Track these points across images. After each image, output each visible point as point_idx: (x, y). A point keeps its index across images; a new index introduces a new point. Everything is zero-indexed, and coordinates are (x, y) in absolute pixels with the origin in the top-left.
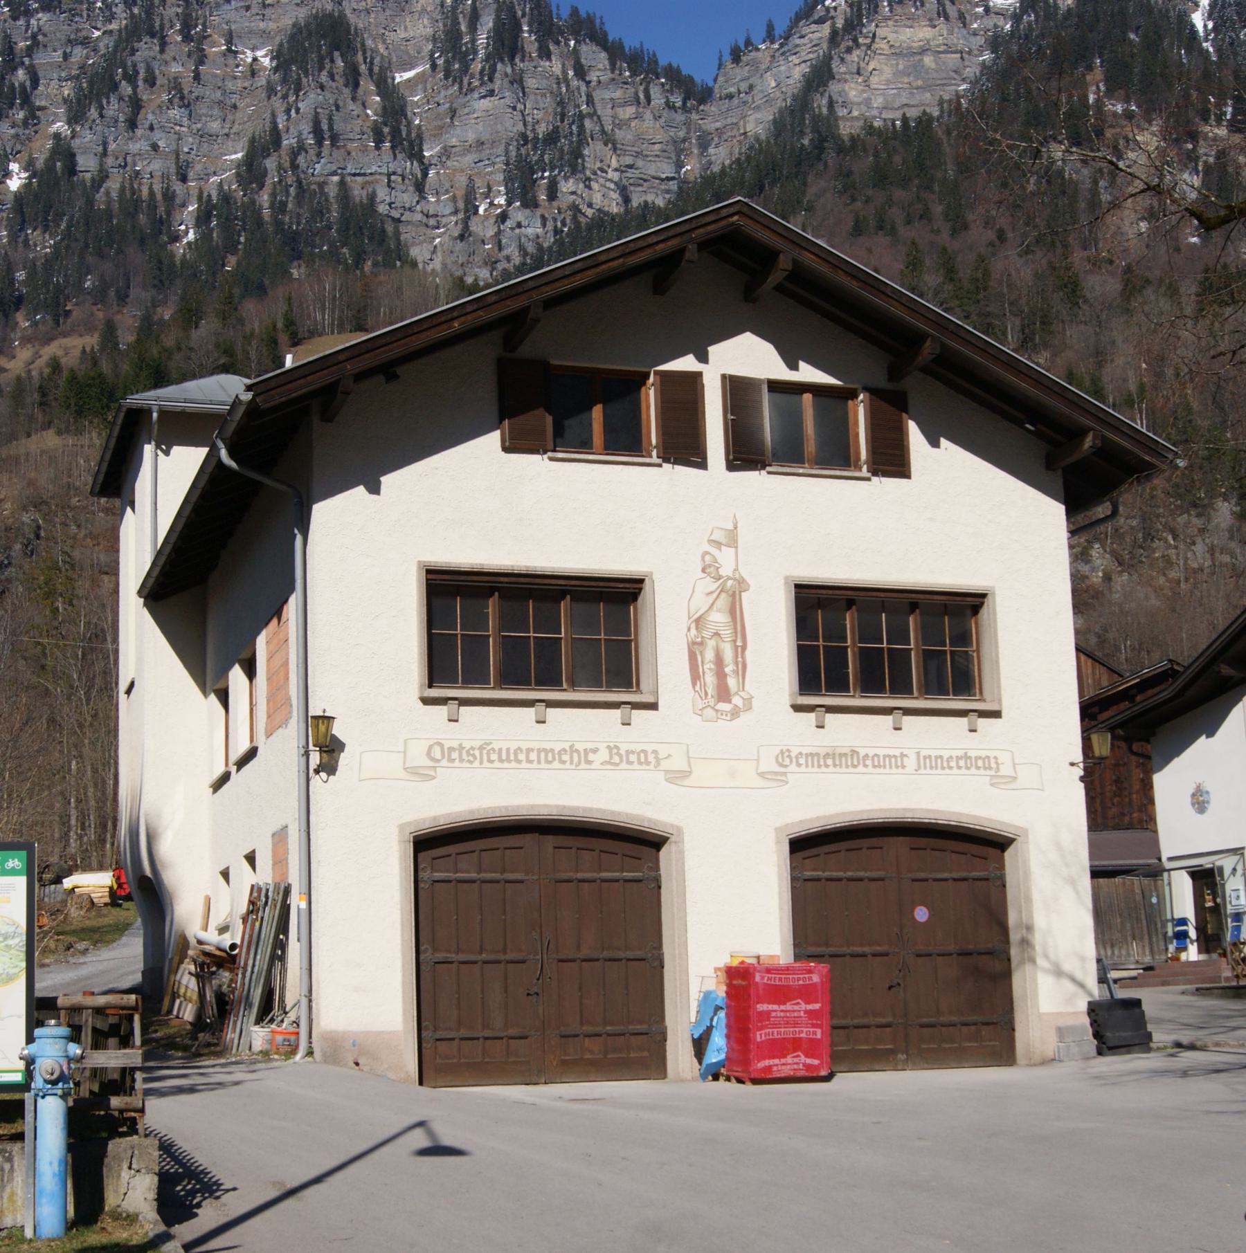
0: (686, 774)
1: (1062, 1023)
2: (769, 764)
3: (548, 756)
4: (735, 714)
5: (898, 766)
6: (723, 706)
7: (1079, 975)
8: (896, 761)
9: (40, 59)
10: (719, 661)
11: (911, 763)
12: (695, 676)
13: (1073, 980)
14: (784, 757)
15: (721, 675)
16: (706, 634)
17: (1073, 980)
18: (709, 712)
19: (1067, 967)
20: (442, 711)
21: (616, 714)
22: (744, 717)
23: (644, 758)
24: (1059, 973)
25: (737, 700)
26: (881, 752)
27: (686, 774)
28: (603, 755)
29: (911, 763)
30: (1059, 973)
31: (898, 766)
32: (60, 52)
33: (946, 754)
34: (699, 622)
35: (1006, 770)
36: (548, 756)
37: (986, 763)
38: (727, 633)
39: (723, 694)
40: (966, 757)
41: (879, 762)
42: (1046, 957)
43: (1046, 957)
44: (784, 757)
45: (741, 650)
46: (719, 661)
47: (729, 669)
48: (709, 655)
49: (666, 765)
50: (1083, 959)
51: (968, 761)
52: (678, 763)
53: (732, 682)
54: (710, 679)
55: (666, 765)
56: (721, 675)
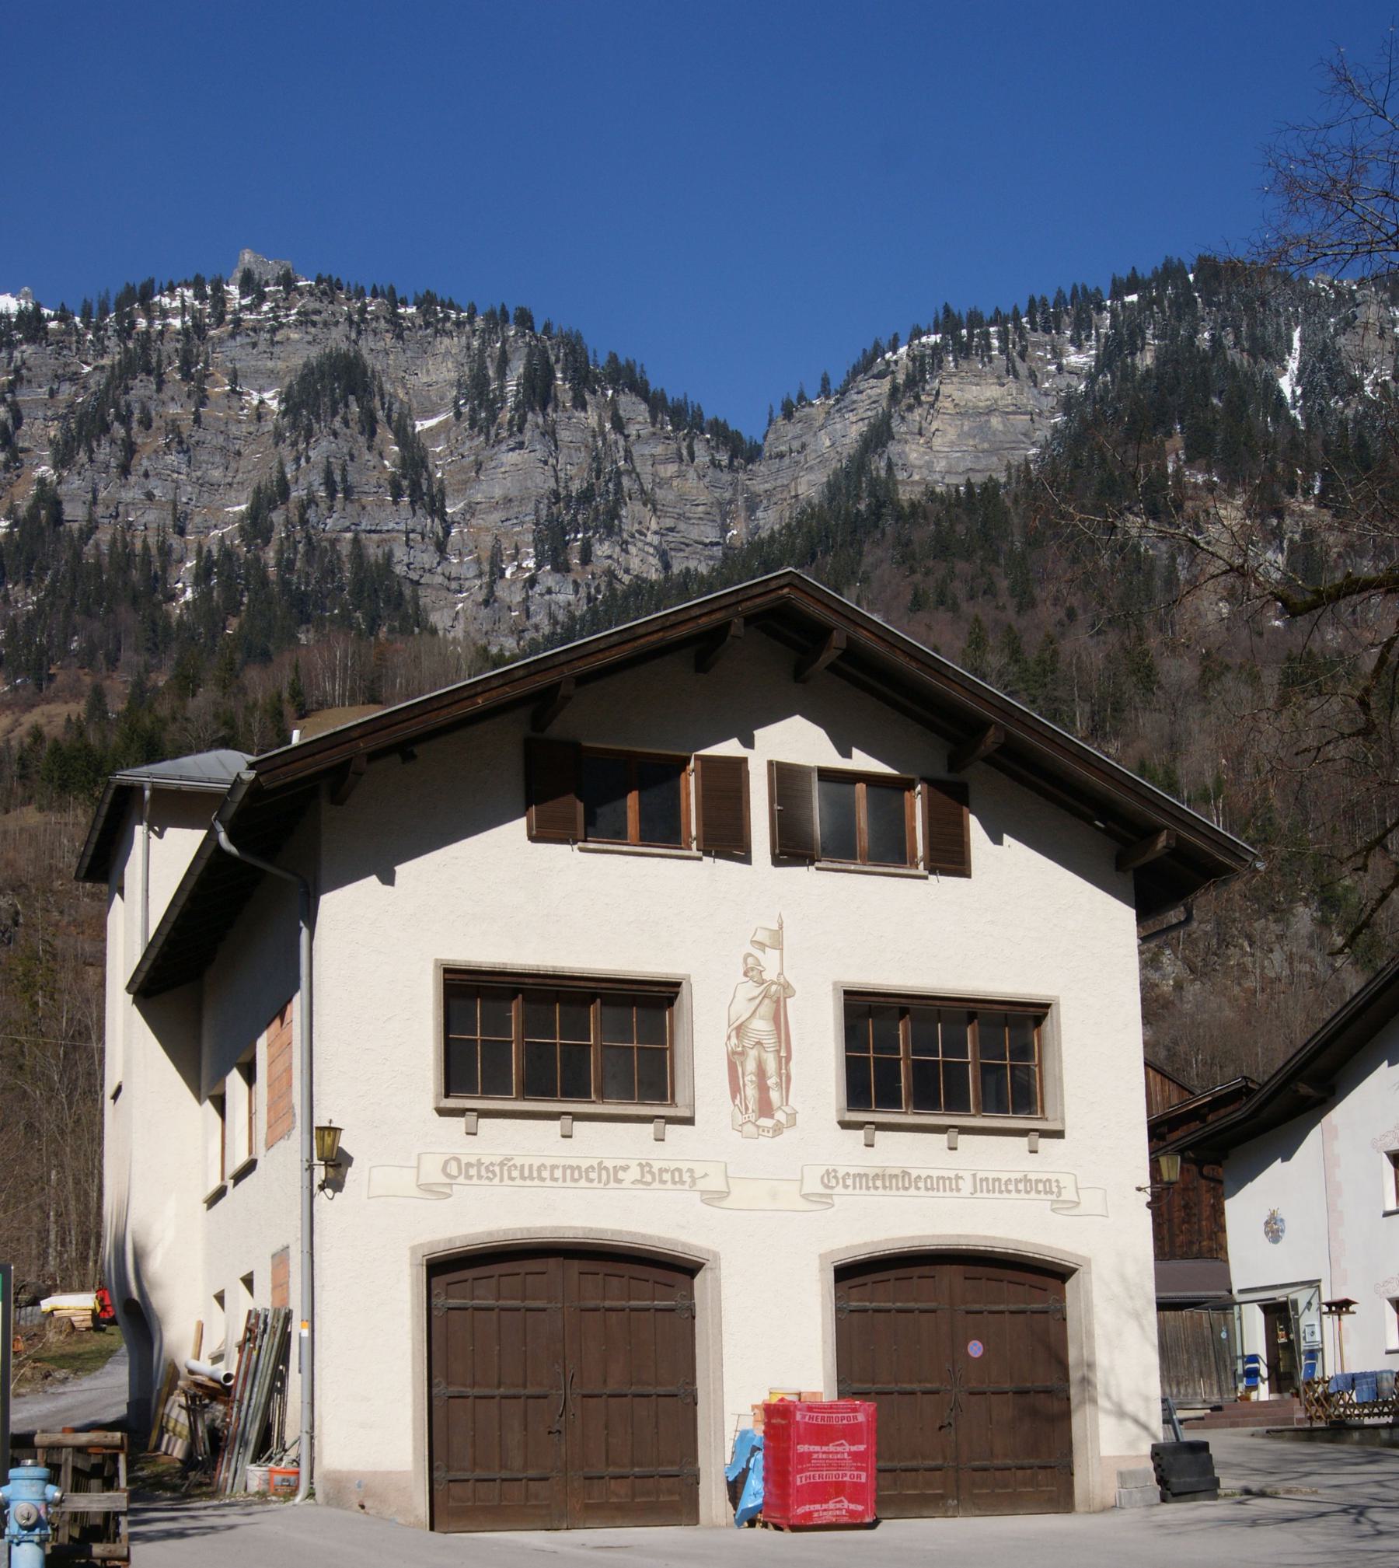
1: (1124, 1467)
2: (814, 1186)
3: (575, 1173)
4: (778, 1130)
5: (952, 1188)
6: (765, 1122)
7: (1143, 1417)
8: (950, 1184)
11: (966, 1186)
12: (735, 1088)
13: (1136, 1421)
14: (830, 1177)
16: (748, 1043)
17: (1136, 1421)
19: (1130, 1407)
20: (459, 1123)
21: (649, 1128)
22: (787, 1134)
23: (678, 1178)
24: (1121, 1414)
25: (780, 1116)
26: (935, 1174)
28: (634, 1173)
29: (966, 1186)
30: (1121, 1414)
31: (952, 1188)
33: (1004, 1177)
34: (740, 1030)
35: (1068, 1194)
36: (575, 1173)
37: (1046, 1187)
38: (770, 1042)
39: (765, 1108)
40: (1026, 1180)
41: (934, 1184)
42: (1108, 1396)
44: (830, 1177)
45: (785, 1060)
47: (771, 1082)
48: (751, 1066)
49: (702, 1185)
50: (1147, 1399)
51: (1027, 1185)
52: (715, 1183)
53: (775, 1096)
54: (751, 1092)
55: (702, 1185)
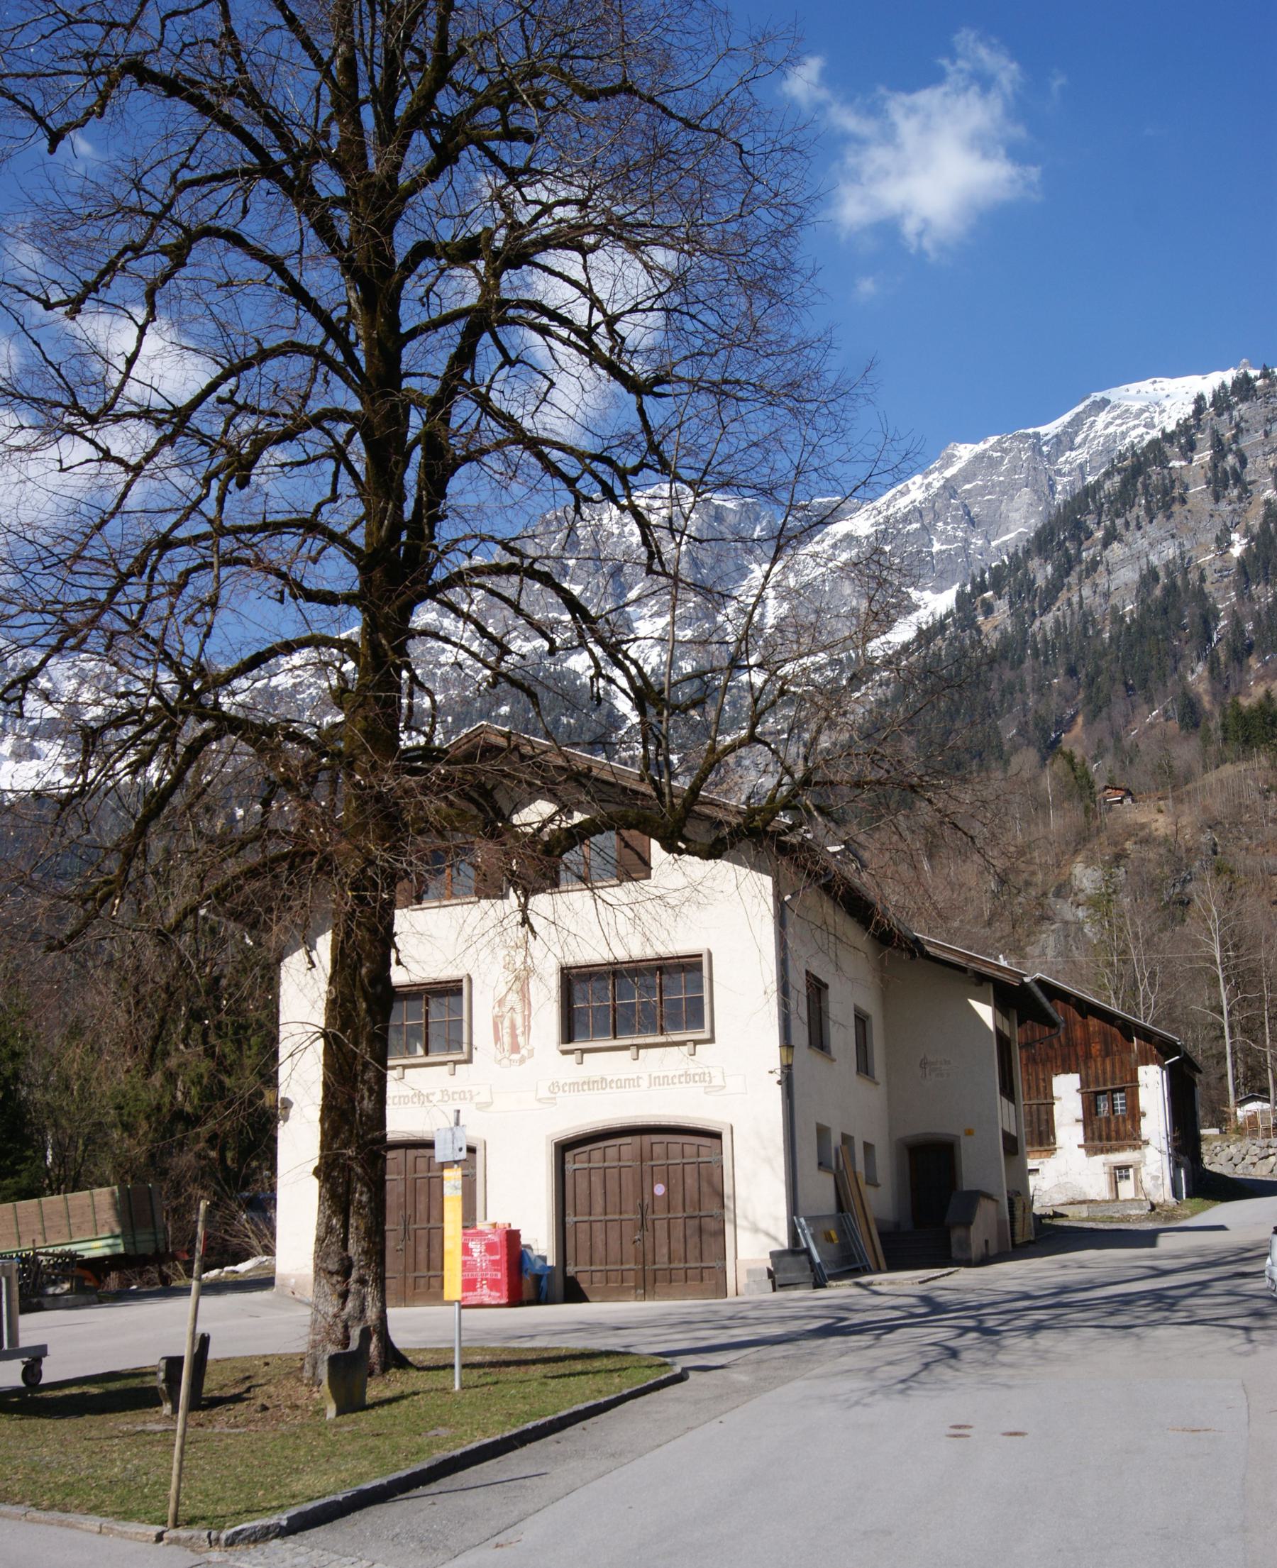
0: (489, 1104)
1: (753, 1266)
2: (544, 1093)
3: (590, 1084)
4: (522, 1061)
5: (637, 1084)
6: (516, 1057)
7: (772, 1231)
8: (634, 1082)
9: (1245, 442)
10: (513, 1027)
11: (644, 1083)
12: (497, 1038)
13: (768, 1234)
14: (554, 1087)
15: (514, 1036)
16: (505, 1009)
17: (768, 1234)
18: (505, 1062)
19: (763, 1225)
20: (572, 1058)
21: (445, 1068)
22: (528, 1062)
23: (703, 1077)
24: (756, 1229)
25: (524, 1052)
26: (623, 1077)
27: (489, 1104)
28: (438, 1096)
29: (644, 1083)
30: (756, 1229)
31: (637, 1084)
32: (1261, 432)
33: (670, 1074)
34: (501, 1002)
35: (717, 1081)
36: (590, 1084)
37: (703, 1077)
38: (519, 1007)
39: (515, 1048)
40: (686, 1074)
41: (621, 1084)
42: (746, 1218)
43: (746, 1218)
44: (554, 1087)
45: (527, 1018)
46: (513, 1027)
47: (519, 1032)
48: (507, 1023)
49: (477, 1099)
50: (776, 1219)
51: (688, 1077)
52: (484, 1098)
53: (521, 1040)
54: (507, 1039)
55: (477, 1099)
56: (514, 1036)
